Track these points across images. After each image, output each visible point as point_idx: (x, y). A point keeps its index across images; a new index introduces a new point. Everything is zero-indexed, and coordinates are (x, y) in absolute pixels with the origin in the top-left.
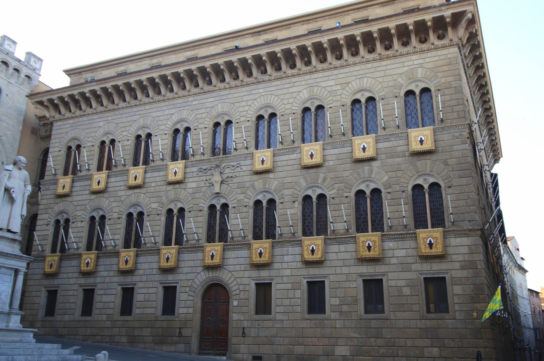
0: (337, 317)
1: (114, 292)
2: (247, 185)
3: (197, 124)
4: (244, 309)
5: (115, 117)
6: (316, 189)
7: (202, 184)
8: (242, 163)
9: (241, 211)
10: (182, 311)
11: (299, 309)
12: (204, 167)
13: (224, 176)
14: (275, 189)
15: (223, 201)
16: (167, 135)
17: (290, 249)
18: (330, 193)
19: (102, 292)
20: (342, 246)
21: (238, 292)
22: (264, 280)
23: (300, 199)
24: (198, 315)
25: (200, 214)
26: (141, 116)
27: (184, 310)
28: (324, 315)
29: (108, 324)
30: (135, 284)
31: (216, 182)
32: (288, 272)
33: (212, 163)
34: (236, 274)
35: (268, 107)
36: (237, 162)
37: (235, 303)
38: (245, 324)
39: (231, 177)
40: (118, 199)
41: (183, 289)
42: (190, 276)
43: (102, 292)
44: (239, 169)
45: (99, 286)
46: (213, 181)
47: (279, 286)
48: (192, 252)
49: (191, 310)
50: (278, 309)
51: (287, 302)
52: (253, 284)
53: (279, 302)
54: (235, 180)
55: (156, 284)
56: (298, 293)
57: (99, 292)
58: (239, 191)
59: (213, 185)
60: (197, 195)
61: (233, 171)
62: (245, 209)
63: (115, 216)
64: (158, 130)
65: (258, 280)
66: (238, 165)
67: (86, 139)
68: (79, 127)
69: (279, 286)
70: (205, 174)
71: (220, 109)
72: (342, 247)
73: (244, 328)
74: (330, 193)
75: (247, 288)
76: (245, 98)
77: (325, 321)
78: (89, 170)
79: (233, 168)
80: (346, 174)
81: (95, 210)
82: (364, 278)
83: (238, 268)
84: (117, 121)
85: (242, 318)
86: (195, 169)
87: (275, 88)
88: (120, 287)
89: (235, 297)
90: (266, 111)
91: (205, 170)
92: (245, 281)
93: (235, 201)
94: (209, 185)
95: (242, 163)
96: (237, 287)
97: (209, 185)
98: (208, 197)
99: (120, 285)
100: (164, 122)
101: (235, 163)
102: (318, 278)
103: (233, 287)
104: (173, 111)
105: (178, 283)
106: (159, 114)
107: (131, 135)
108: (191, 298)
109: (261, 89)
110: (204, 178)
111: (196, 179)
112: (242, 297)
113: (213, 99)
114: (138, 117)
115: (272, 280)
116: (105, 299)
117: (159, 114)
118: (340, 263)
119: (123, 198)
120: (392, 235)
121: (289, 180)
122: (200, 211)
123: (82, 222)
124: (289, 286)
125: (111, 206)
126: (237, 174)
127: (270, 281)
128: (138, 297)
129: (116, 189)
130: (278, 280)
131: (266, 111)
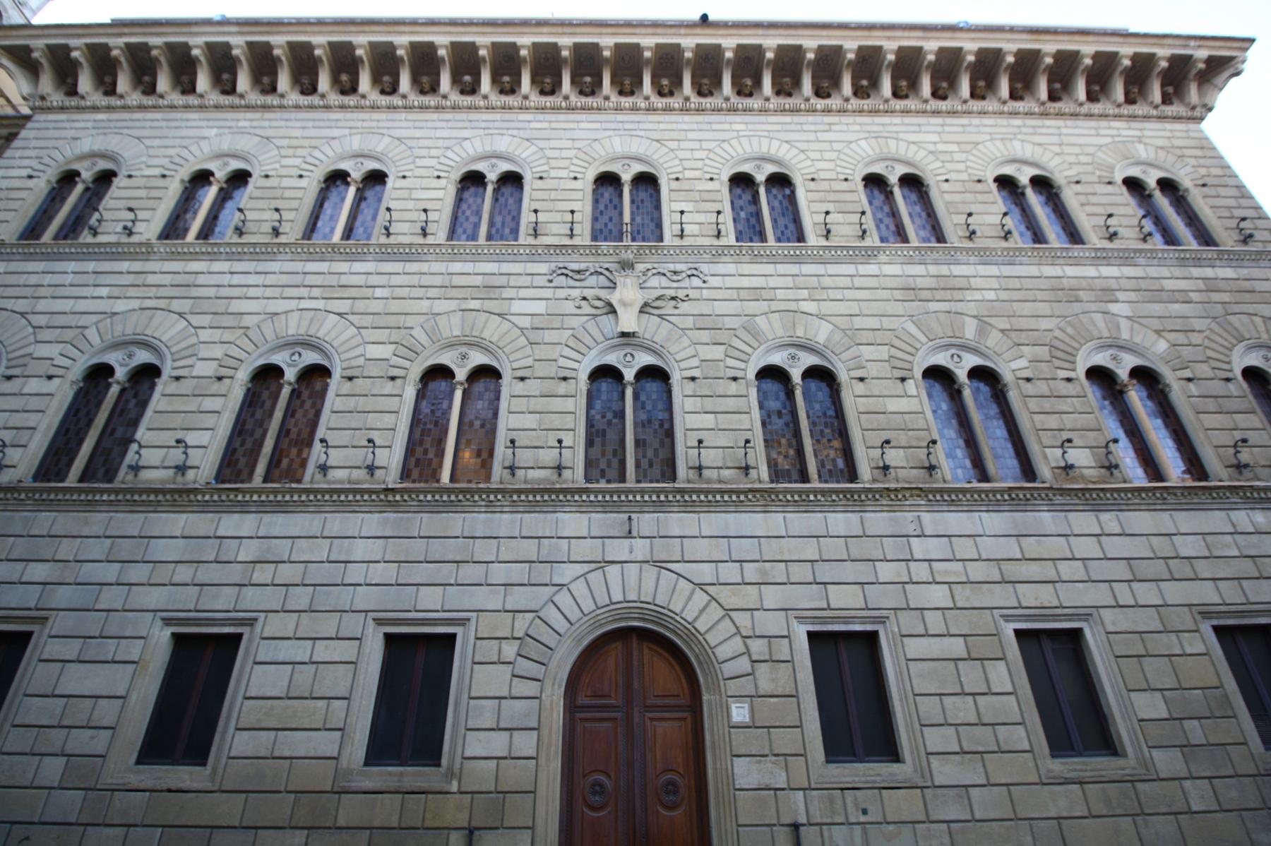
0: (1180, 768)
1: (134, 650)
2: (730, 322)
3: (545, 168)
4: (785, 740)
5: (266, 124)
6: (962, 354)
7: (569, 307)
8: (704, 268)
9: (720, 391)
10: (476, 745)
11: (1017, 737)
12: (575, 266)
13: (651, 295)
14: (828, 339)
15: (645, 359)
16: (443, 182)
17: (926, 517)
18: (1014, 365)
19: (70, 649)
20: (1105, 516)
21: (743, 665)
22: (847, 620)
23: (918, 374)
24: (553, 766)
25: (562, 388)
27: (497, 744)
28: (1121, 762)
29: (70, 803)
30: (251, 622)
31: (625, 304)
32: (939, 595)
33: (601, 259)
34: (723, 594)
35: (763, 159)
37: (739, 713)
38: (797, 808)
39: (673, 298)
40: (228, 321)
41: (488, 650)
42: (519, 598)
43: (70, 649)
44: (696, 282)
45: (61, 623)
46: (615, 298)
47: (915, 647)
48: (533, 507)
49: (525, 744)
50: (936, 739)
51: (962, 709)
52: (801, 633)
53: (929, 708)
54: (685, 307)
55: (353, 624)
56: (1000, 676)
57: (55, 649)
58: (705, 336)
59: (615, 312)
60: (549, 336)
61: (675, 285)
62: (733, 388)
63: (207, 369)
64: (412, 167)
65: (823, 620)
66: (695, 272)
67: (144, 159)
68: (125, 131)
69: (915, 647)
70: (578, 284)
71: (619, 145)
72: (1110, 521)
73: (796, 827)
74: (1014, 365)
75: (782, 651)
77: (1140, 786)
78: (130, 233)
79: (675, 278)
80: (1045, 324)
81: (116, 346)
82: (1215, 622)
83: (730, 572)
85: (781, 781)
86: (543, 268)
87: (779, 127)
88: (168, 632)
89: (732, 687)
91: (579, 272)
92: (772, 624)
93: (695, 362)
94: (594, 311)
95: (704, 268)
96: (736, 645)
97: (594, 311)
98: (592, 344)
99: (168, 622)
100: (434, 152)
101: (679, 267)
102: (1055, 618)
103: (722, 643)
105: (463, 622)
108: (531, 688)
109: (738, 123)
110: (576, 293)
111: (548, 293)
112: (765, 686)
113: (598, 126)
114: (347, 131)
115: (882, 620)
116: (79, 680)
118: (1121, 571)
119: (248, 321)
120: (1259, 489)
121: (873, 323)
122: (565, 379)
123: (50, 377)
124: (957, 647)
125: (194, 340)
126: (693, 293)
127: (869, 628)
128: (256, 679)
129: (225, 292)
130: (908, 622)
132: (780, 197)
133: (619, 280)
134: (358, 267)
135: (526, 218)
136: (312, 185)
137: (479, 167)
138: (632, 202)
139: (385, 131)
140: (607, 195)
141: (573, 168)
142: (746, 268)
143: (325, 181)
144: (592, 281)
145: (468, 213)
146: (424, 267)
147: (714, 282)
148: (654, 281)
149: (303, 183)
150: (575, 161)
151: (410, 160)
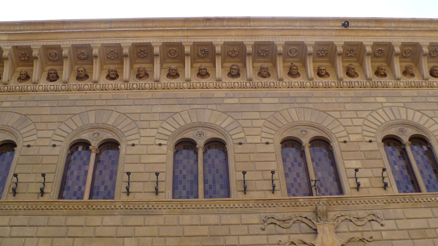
3: (242, 135)
5: (23, 104)
8: (379, 213)
12: (279, 216)
16: (164, 148)
26: (89, 108)
33: (300, 209)
36: (369, 212)
44: (376, 226)
61: (360, 229)
64: (137, 136)
66: (374, 218)
70: (284, 231)
76: (348, 107)
79: (359, 223)
84: (26, 111)
86: (255, 219)
90: (402, 131)
100: (153, 124)
101: (361, 214)
104: (176, 109)
106: (139, 109)
107: (62, 139)
114: (83, 109)
117: (139, 109)
126: (376, 236)
131: (402, 131)
132: (421, 153)
133: (320, 228)
134: (107, 220)
135: (235, 177)
136: (62, 151)
137: (190, 135)
138: (313, 160)
139: (113, 108)
140: (291, 155)
141: (263, 135)
142: (410, 213)
143: (70, 148)
144: (295, 228)
145: (184, 172)
146: (160, 220)
147: (390, 224)
148: (343, 227)
149: (56, 151)
150: (264, 129)
151: (135, 131)
